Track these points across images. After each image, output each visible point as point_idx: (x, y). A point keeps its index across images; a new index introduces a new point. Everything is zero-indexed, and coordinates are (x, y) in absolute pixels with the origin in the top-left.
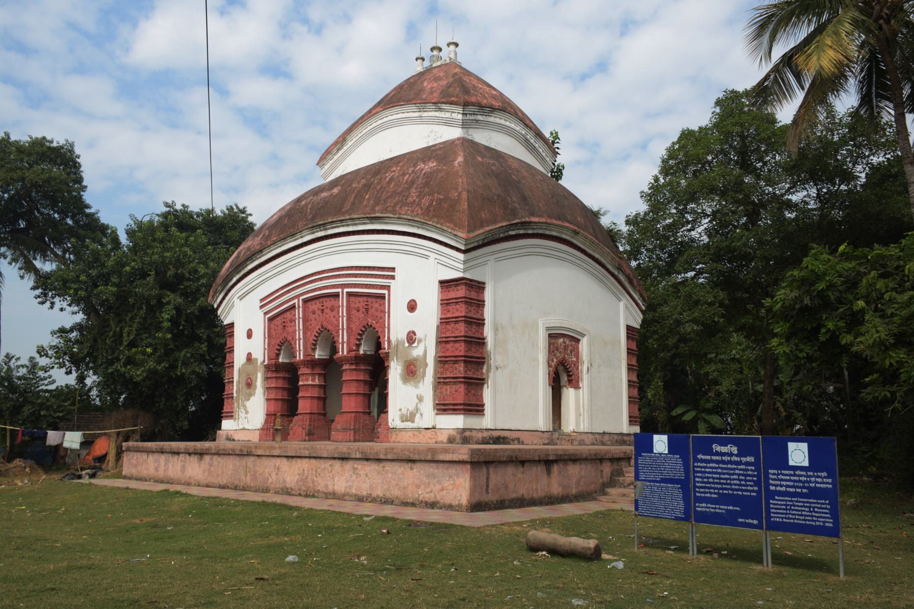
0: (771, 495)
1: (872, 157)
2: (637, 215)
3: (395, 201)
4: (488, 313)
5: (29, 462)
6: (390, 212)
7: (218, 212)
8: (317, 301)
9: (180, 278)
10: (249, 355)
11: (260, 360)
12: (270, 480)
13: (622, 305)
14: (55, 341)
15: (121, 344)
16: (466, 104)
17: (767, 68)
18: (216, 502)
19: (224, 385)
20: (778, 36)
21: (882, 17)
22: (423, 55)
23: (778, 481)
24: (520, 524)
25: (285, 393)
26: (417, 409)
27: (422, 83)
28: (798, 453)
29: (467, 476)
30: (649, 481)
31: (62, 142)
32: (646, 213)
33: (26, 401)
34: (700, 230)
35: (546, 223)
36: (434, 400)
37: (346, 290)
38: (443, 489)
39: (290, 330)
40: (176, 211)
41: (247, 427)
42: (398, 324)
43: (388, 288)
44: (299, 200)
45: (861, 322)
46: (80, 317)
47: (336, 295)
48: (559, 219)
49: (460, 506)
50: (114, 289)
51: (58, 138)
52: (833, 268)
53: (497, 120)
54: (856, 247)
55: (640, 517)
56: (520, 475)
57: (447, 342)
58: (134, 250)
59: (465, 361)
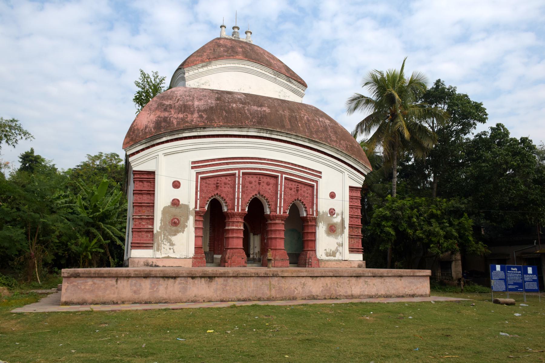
8: (255, 176)
11: (192, 206)
12: (296, 292)
23: (527, 278)
26: (337, 250)
28: (530, 270)
37: (284, 176)
41: (171, 256)
42: (323, 204)
43: (317, 182)
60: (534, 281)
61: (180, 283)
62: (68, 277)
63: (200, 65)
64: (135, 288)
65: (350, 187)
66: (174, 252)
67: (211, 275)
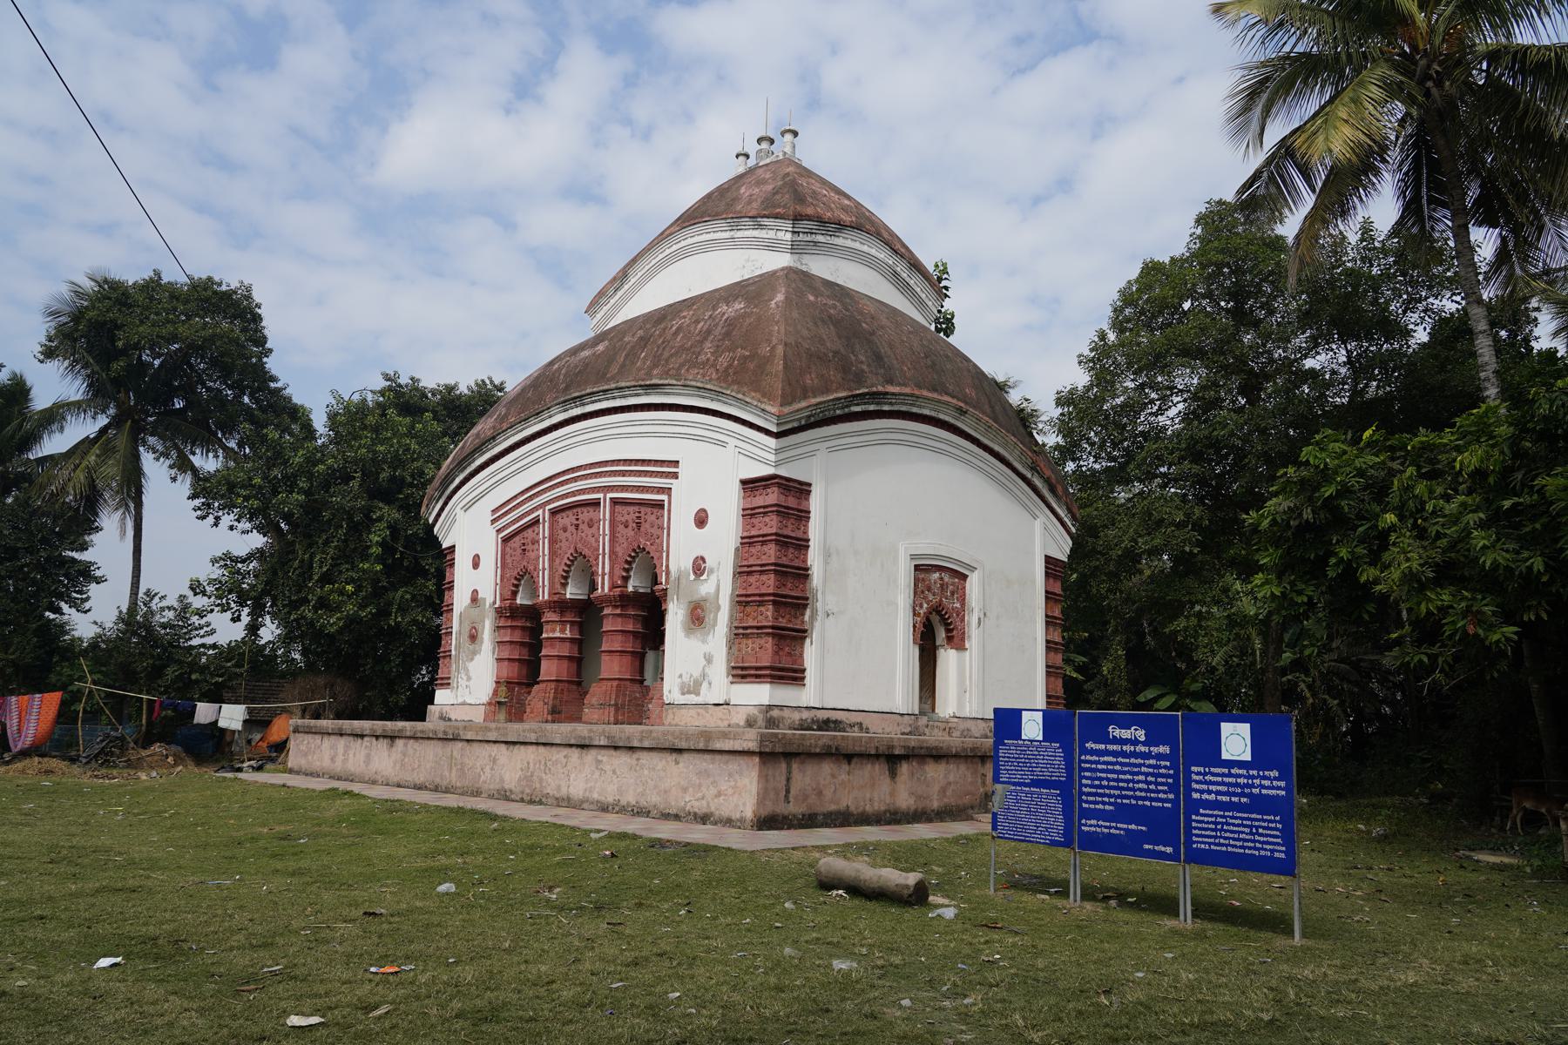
0: (1194, 806)
1: (1431, 300)
2: (1073, 391)
3: (681, 360)
4: (815, 530)
5: (174, 748)
6: (672, 377)
7: (463, 389)
8: (570, 513)
9: (398, 483)
10: (475, 592)
11: (489, 600)
13: (1038, 525)
14: (217, 572)
15: (311, 579)
16: (797, 218)
17: (1257, 160)
18: (393, 806)
19: (439, 638)
20: (1274, 110)
21: (1430, 78)
22: (746, 150)
23: (1205, 784)
24: (823, 849)
25: (525, 651)
26: (704, 675)
27: (739, 189)
28: (1236, 740)
29: (755, 774)
30: (1015, 784)
31: (234, 285)
32: (1088, 389)
33: (171, 660)
34: (1172, 412)
35: (912, 395)
36: (728, 661)
38: (719, 794)
39: (532, 555)
40: (400, 386)
42: (682, 545)
43: (668, 491)
44: (552, 363)
45: (1385, 546)
46: (257, 540)
47: (596, 504)
48: (935, 390)
49: (742, 820)
50: (302, 498)
51: (230, 280)
52: (1349, 463)
53: (849, 243)
54: (1391, 433)
55: (999, 841)
56: (844, 777)
57: (749, 573)
58: (337, 440)
59: (775, 603)
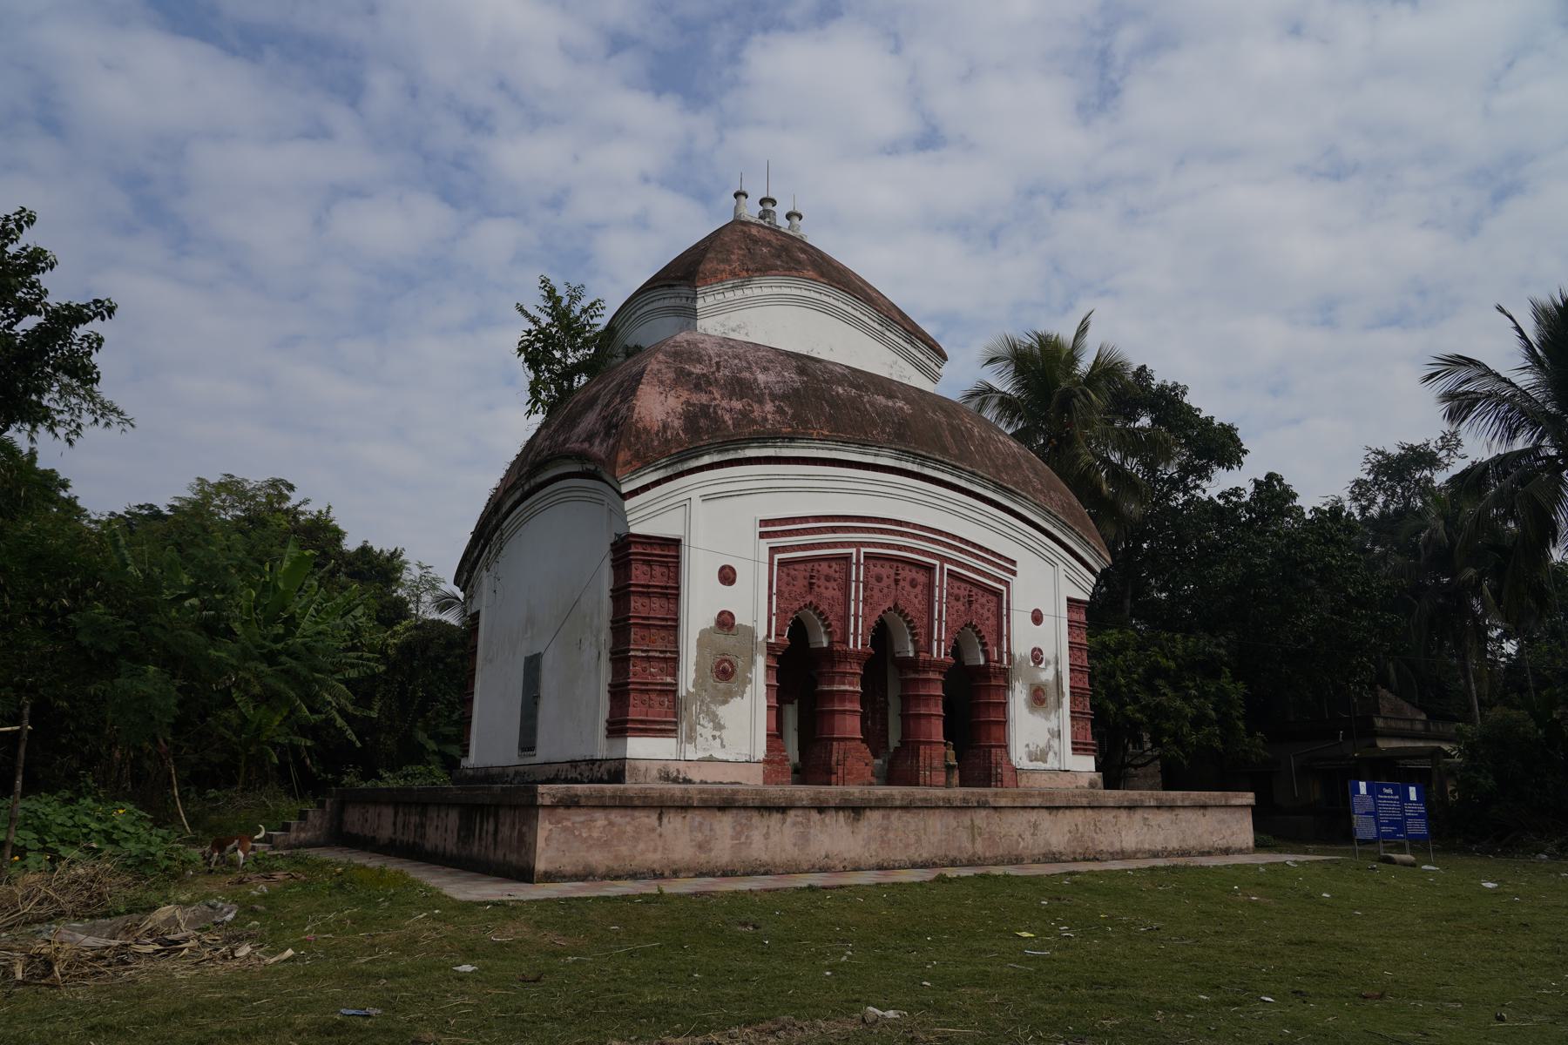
8: (887, 564)
11: (762, 632)
37: (947, 566)
42: (1022, 637)
43: (1007, 584)
60: (1420, 816)
61: (794, 824)
62: (553, 807)
63: (729, 284)
64: (700, 837)
65: (1069, 600)
66: (723, 746)
67: (858, 804)
